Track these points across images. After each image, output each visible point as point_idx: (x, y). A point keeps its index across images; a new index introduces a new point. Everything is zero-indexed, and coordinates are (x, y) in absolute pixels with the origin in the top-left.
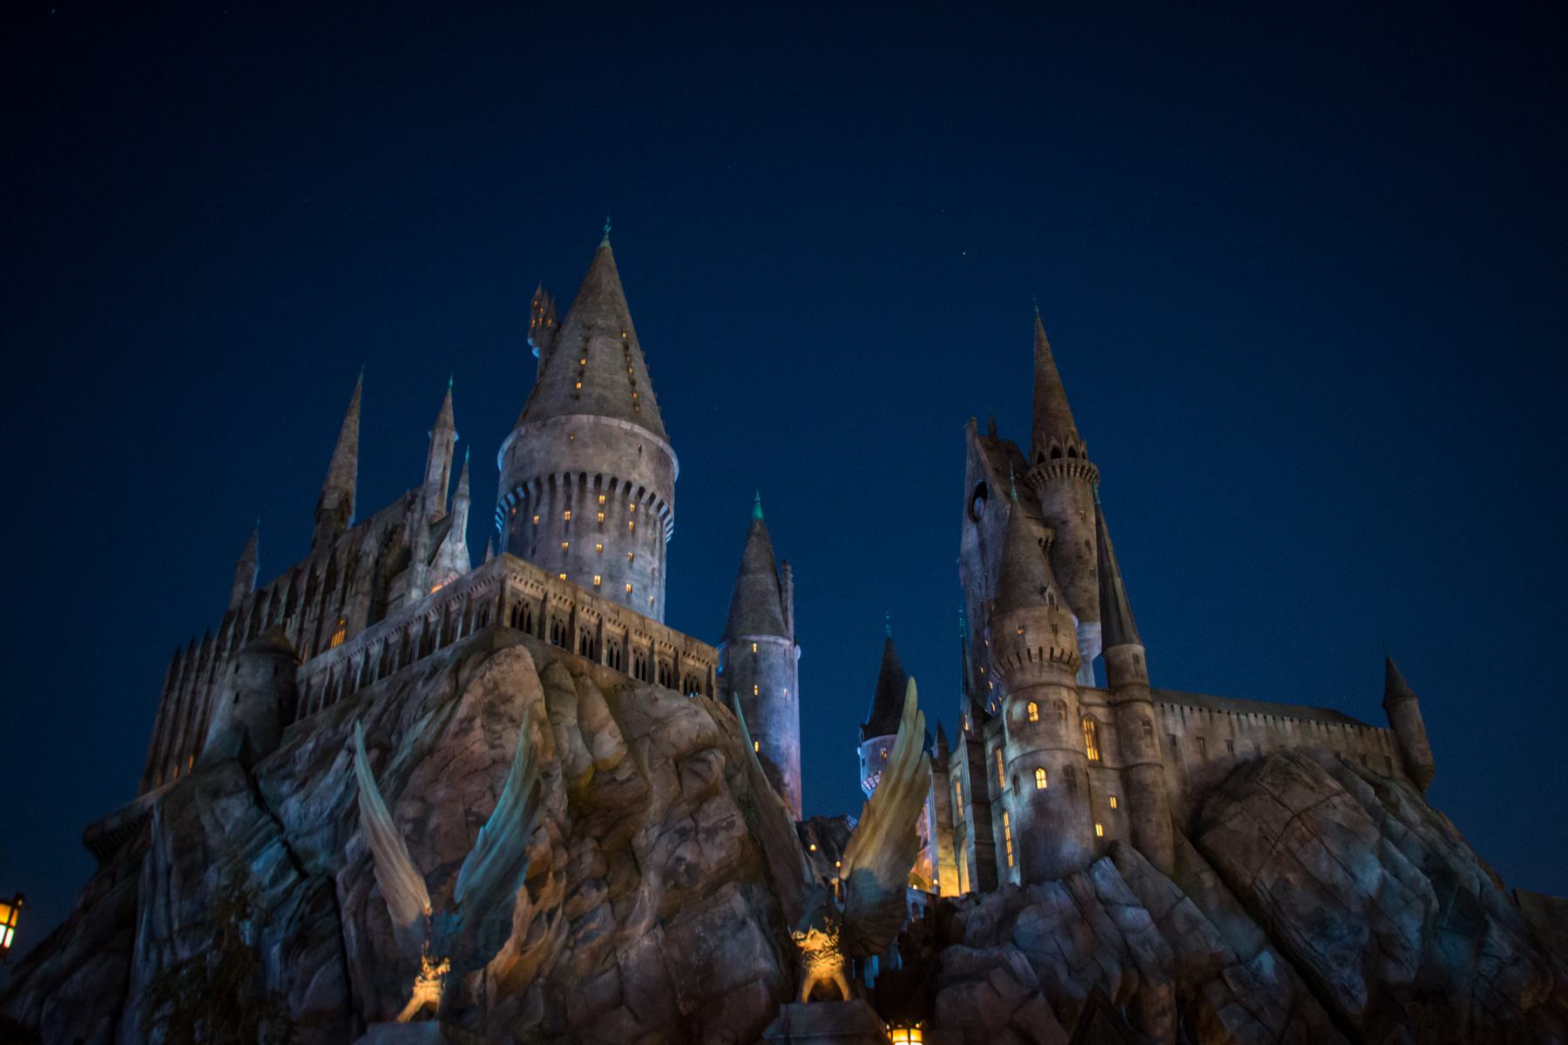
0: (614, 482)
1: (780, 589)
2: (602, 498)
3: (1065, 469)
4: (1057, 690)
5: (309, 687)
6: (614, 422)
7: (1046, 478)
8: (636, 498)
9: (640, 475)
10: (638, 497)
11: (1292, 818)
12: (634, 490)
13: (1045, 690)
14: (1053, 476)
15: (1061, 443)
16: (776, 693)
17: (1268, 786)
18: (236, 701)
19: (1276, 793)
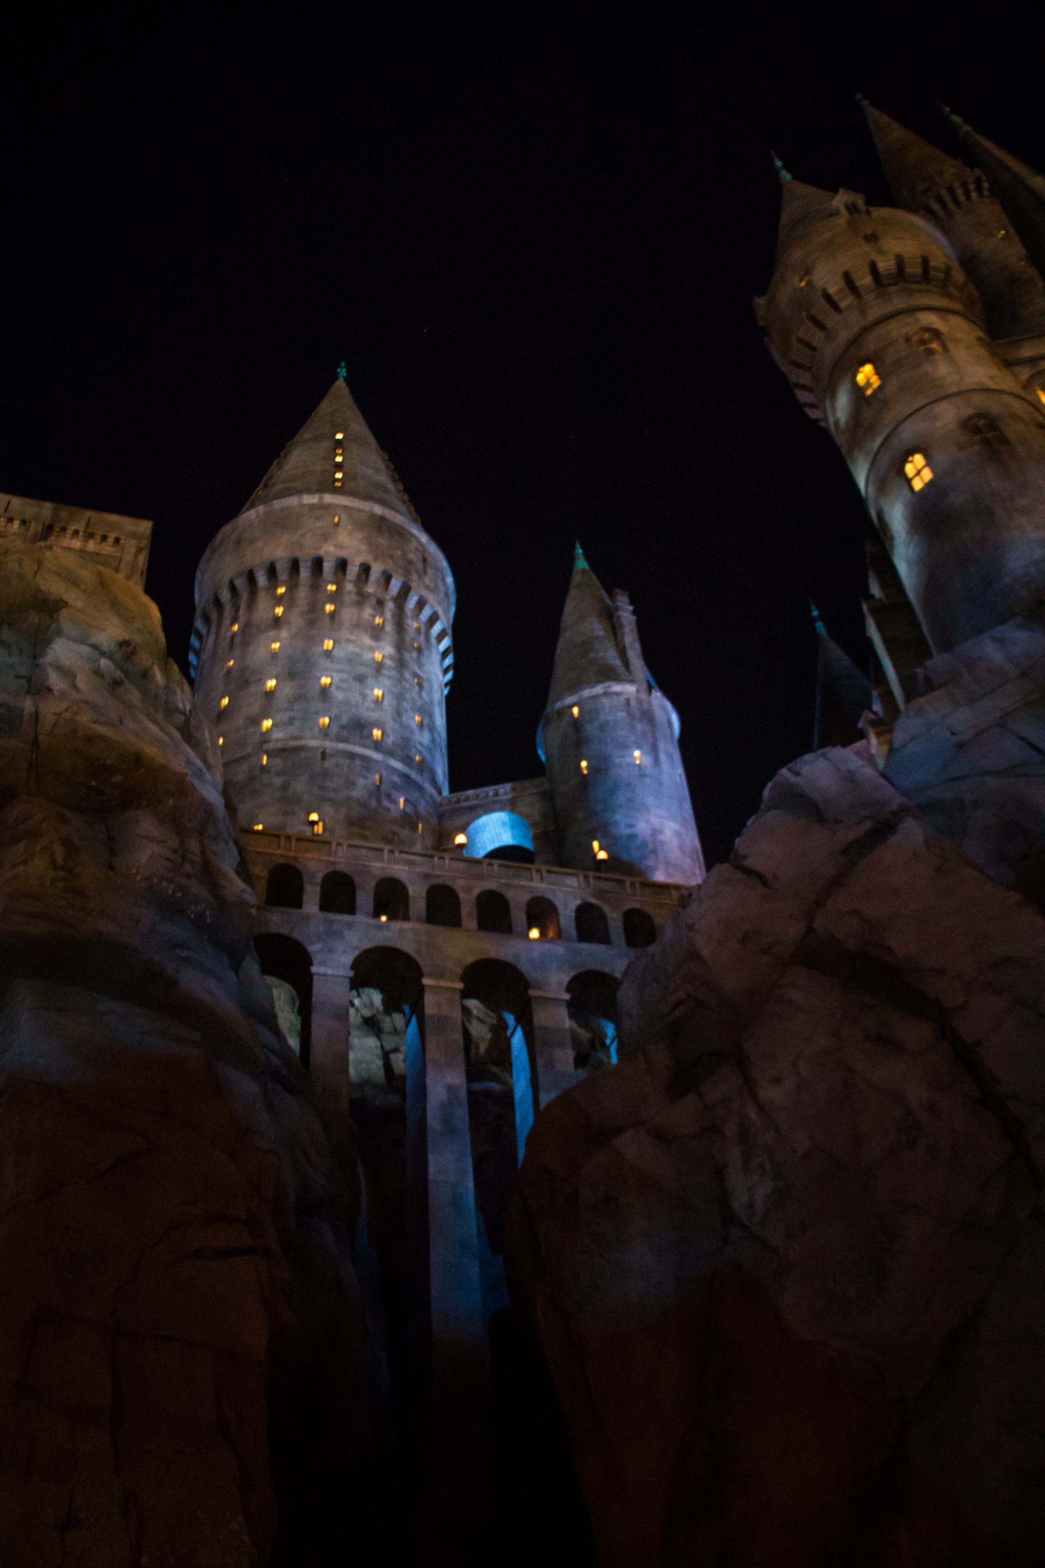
0: (295, 566)
1: (614, 628)
2: (281, 590)
3: (947, 198)
4: (909, 320)
6: (293, 501)
8: (336, 573)
10: (340, 574)
12: (328, 566)
13: (880, 331)
16: (618, 760)
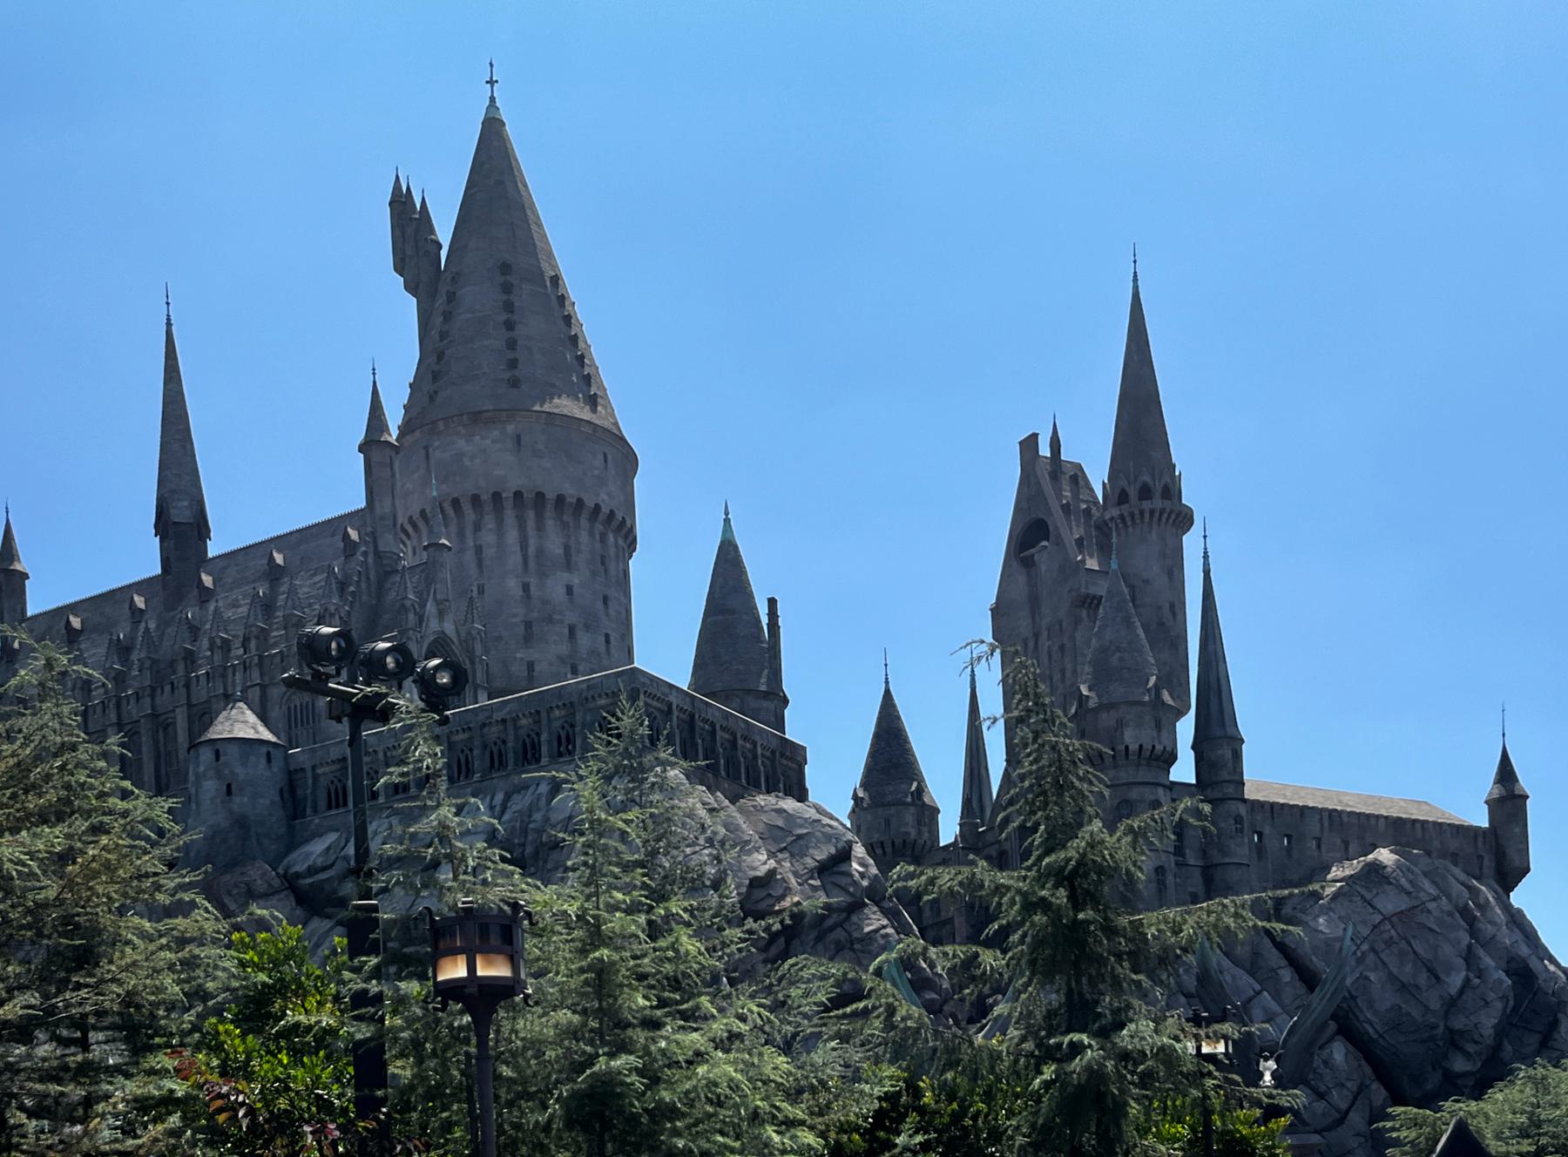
5: (316, 777)
7: (1129, 523)
9: (609, 494)
11: (1382, 921)
14: (1138, 521)
15: (1154, 481)
17: (1359, 889)
18: (229, 791)
19: (1368, 896)
